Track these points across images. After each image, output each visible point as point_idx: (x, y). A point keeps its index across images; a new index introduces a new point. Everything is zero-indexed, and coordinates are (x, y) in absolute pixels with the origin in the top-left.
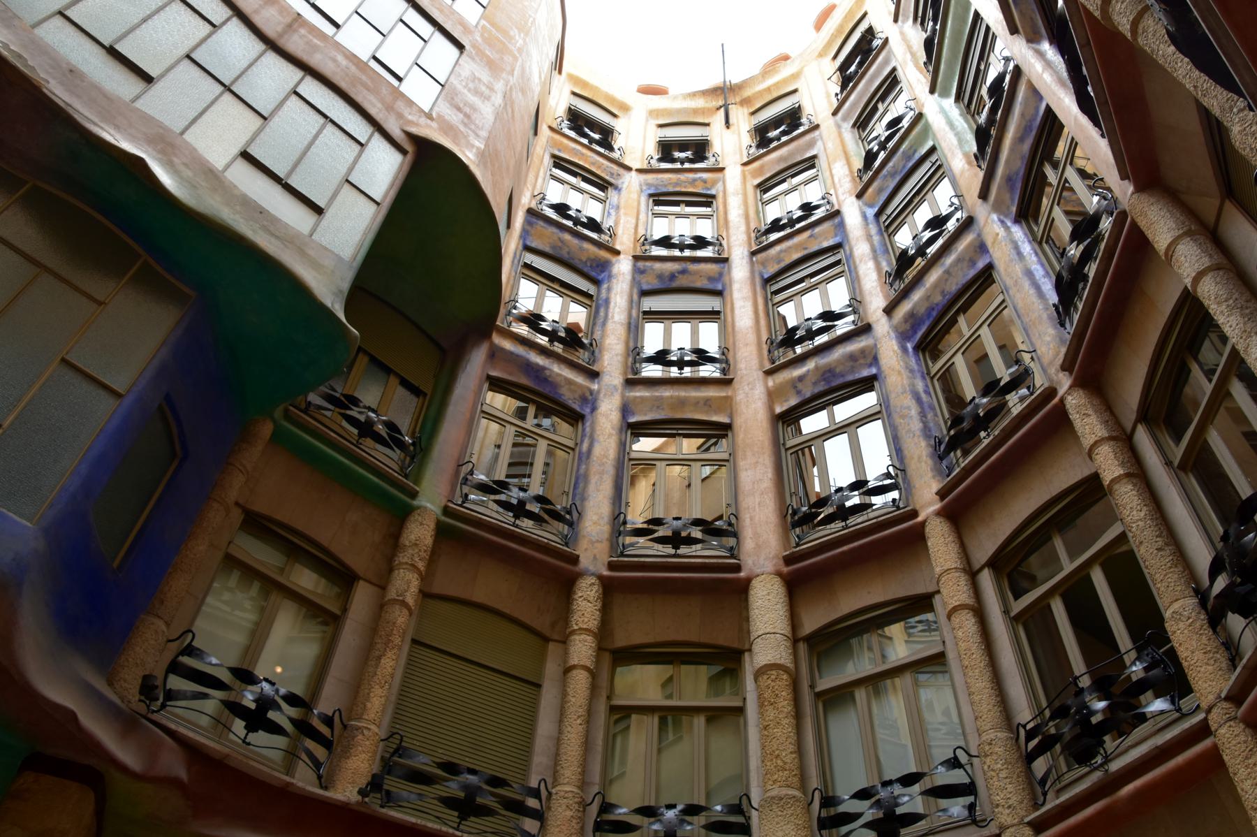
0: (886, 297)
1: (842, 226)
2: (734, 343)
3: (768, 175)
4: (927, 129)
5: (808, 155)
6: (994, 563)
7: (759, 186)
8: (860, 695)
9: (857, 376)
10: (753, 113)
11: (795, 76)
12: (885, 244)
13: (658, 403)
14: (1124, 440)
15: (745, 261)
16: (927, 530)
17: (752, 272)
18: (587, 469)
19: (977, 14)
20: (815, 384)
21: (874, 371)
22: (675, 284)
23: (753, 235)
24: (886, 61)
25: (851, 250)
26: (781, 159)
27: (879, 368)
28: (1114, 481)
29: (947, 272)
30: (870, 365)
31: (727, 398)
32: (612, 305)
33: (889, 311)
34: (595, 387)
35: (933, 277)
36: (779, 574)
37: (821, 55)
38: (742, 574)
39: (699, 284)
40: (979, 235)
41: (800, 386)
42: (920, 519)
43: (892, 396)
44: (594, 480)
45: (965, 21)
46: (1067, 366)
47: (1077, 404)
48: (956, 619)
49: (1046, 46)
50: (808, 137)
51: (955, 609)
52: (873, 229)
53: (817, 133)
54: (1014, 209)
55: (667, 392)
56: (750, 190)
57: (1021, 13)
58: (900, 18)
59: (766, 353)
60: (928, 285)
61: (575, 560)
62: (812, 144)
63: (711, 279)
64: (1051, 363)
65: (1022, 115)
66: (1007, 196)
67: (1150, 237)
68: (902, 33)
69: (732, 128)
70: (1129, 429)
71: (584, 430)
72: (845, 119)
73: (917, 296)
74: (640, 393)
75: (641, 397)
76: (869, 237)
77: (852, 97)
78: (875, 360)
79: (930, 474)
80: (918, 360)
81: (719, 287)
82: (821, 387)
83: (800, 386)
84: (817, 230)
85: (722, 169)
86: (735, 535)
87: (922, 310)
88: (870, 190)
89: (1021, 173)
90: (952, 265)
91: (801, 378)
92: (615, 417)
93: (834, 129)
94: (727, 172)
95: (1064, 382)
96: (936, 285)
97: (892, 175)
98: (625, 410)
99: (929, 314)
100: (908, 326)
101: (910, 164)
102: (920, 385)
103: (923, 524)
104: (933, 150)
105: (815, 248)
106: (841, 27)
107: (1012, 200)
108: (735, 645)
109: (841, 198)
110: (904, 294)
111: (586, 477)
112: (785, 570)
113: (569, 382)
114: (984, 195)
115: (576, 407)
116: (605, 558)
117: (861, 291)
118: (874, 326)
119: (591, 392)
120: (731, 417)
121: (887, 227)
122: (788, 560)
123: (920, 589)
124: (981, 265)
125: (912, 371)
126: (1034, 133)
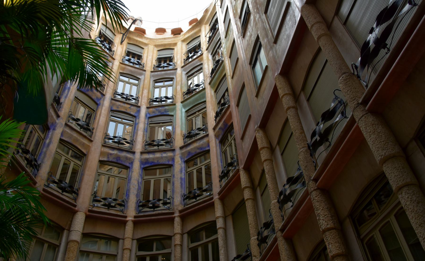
0: (142, 147)
1: (139, 112)
2: (97, 128)
3: (125, 72)
4: (174, 109)
5: (138, 76)
6: (138, 240)
7: (120, 73)
8: (91, 256)
9: (125, 164)
10: (129, 43)
11: (146, 45)
12: (147, 129)
13: (71, 136)
14: (182, 235)
15: (110, 100)
16: (128, 223)
17: (110, 105)
18: (46, 151)
19: (205, 101)
20: (114, 158)
21: (130, 166)
22: (87, 93)
23: (114, 92)
24: (173, 74)
25: (138, 123)
26: (131, 71)
27: (132, 165)
28: (177, 244)
29: (162, 157)
30: (130, 163)
31: (89, 146)
32: (70, 91)
33: (142, 153)
34: (57, 121)
35: (158, 155)
36: (86, 214)
37: (156, 46)
38: (76, 209)
39: (94, 97)
40: (174, 156)
41: (110, 156)
42: (127, 219)
43: (133, 179)
44: (47, 156)
45: (201, 100)
46: (180, 212)
47: (177, 220)
48: (126, 251)
49: (218, 142)
50: (141, 71)
51: (127, 249)
52: (146, 122)
53: (144, 72)
54: (186, 159)
55: (75, 135)
56: (118, 73)
57: (218, 132)
58: (183, 68)
59: (104, 137)
60: (155, 156)
61: (35, 183)
62: (141, 74)
63: (97, 98)
64: (176, 206)
65: (202, 145)
66: (186, 155)
67: (216, 210)
68: (182, 73)
69: (122, 46)
70: (184, 232)
71: (48, 135)
72: (153, 76)
73: (151, 156)
74: (68, 130)
75: (67, 132)
76: (145, 123)
77: (159, 73)
78: (132, 163)
79: (134, 209)
80: (142, 172)
81: (98, 103)
82: (115, 160)
83: (110, 156)
84: (132, 107)
85: (114, 59)
86: (77, 194)
87: (150, 161)
88: (151, 109)
89: (193, 154)
90: (164, 157)
91: (111, 154)
92: (59, 135)
93: (149, 77)
94: (115, 61)
95: (177, 214)
96: (158, 158)
97: (159, 112)
98: (62, 134)
99: (151, 163)
100: (145, 161)
101: (165, 113)
102: (140, 180)
103: (127, 221)
104: (172, 116)
105: (128, 111)
106: (165, 45)
107: (187, 157)
108: (64, 227)
109: (143, 103)
110: (149, 152)
111: (45, 154)
112: (88, 213)
113: (52, 116)
114: (181, 148)
115: (49, 125)
116: (43, 187)
117: (136, 139)
118: (136, 153)
119: (56, 122)
120: (88, 152)
121: (150, 124)
122: (90, 211)
123: (118, 236)
124: (170, 163)
125: (140, 175)
126: (202, 151)
